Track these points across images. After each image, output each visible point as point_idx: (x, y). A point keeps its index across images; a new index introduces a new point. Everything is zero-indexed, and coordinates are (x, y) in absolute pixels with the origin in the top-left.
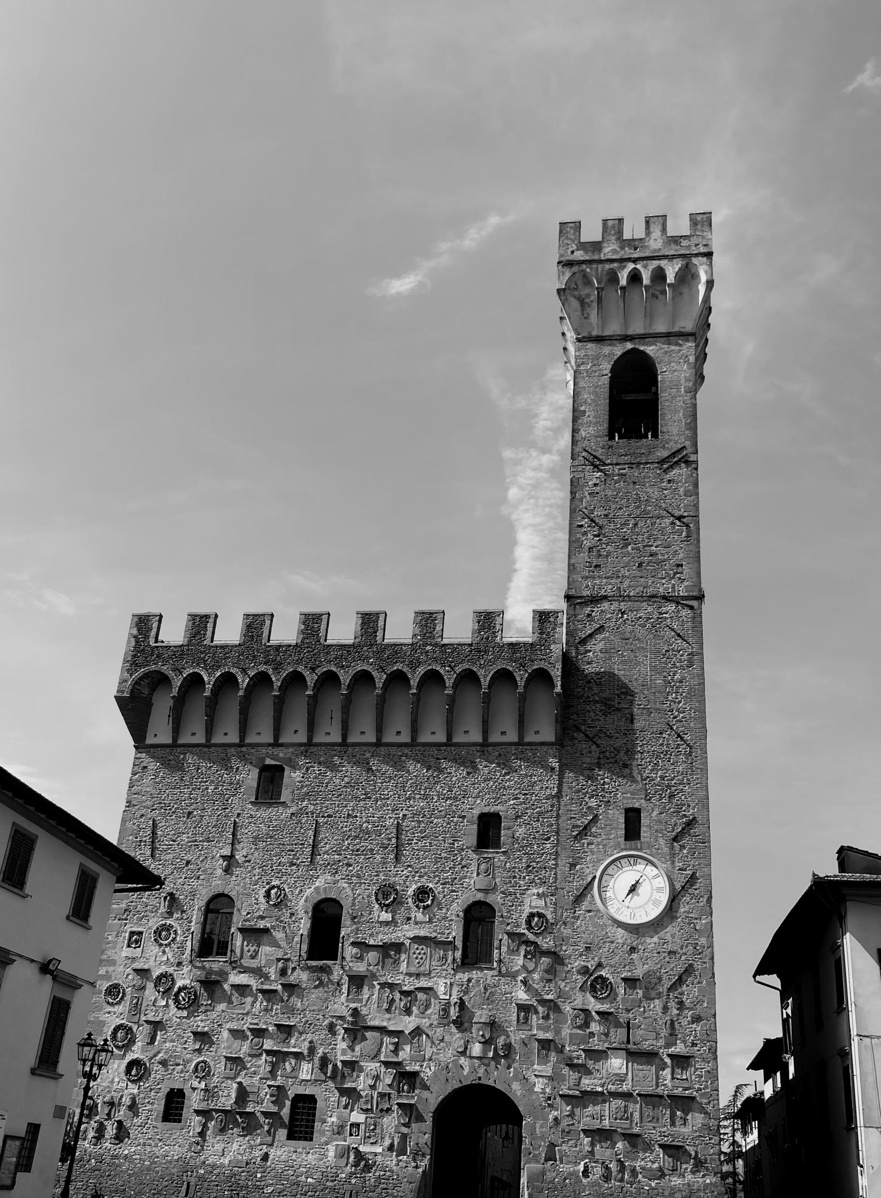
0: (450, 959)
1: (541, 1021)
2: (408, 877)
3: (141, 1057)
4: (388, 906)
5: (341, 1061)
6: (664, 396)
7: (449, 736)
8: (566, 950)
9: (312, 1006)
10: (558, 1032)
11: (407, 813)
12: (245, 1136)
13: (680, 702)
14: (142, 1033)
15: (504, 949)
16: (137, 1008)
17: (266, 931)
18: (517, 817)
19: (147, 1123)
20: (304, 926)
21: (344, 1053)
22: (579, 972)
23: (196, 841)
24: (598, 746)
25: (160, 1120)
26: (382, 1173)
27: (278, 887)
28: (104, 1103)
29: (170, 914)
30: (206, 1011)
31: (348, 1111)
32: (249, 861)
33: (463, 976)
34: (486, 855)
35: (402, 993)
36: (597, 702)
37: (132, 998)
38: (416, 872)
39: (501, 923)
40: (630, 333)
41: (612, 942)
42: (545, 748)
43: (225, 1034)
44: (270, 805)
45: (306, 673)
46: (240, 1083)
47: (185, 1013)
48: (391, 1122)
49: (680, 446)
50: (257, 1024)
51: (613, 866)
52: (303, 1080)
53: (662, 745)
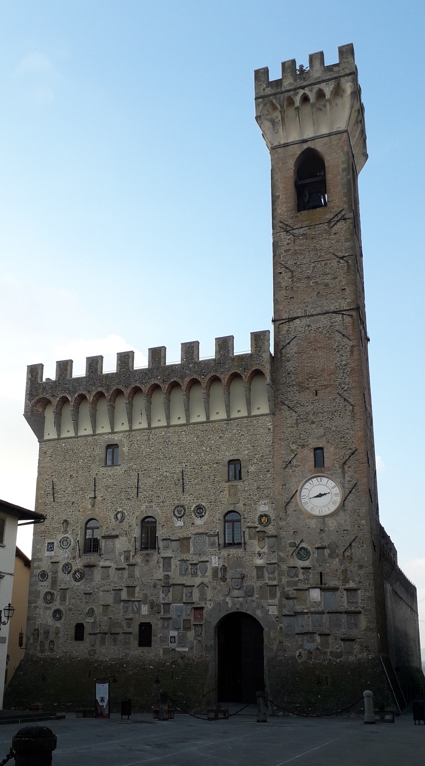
5: (162, 604)
6: (329, 176)
7: (208, 417)
13: (345, 378)
20: (137, 532)
21: (164, 599)
24: (296, 412)
27: (121, 512)
29: (66, 531)
32: (104, 499)
33: (225, 552)
35: (191, 564)
36: (294, 385)
37: (52, 578)
39: (245, 522)
40: (305, 137)
42: (264, 418)
45: (123, 390)
49: (340, 209)
51: (308, 483)
53: (335, 406)
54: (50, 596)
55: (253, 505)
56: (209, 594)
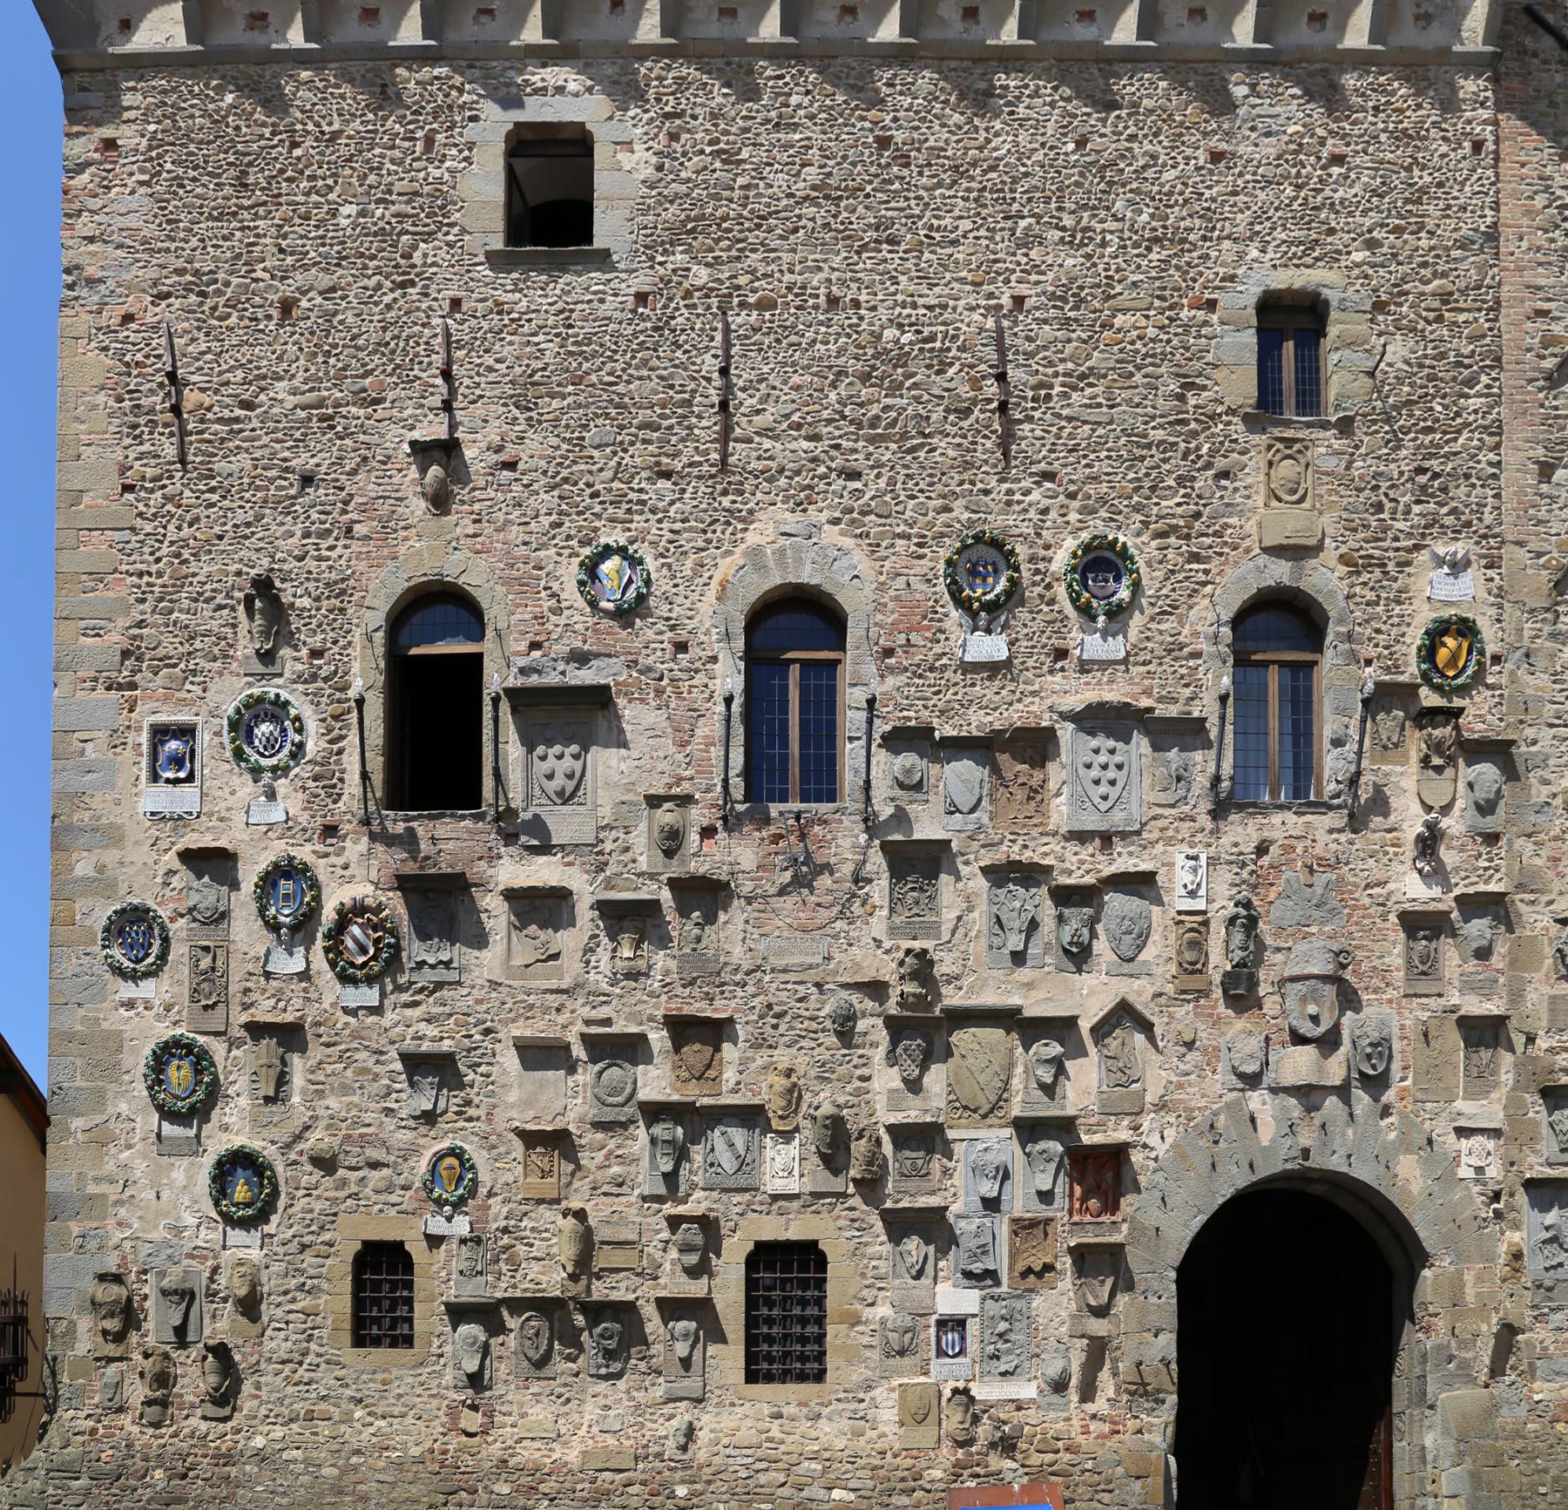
0: (1201, 781)
1: (1472, 965)
2: (1045, 511)
3: (257, 1145)
4: (993, 607)
5: (890, 1129)
9: (781, 953)
10: (1516, 996)
11: (1023, 290)
12: (619, 1376)
14: (239, 1069)
16: (209, 987)
17: (599, 698)
18: (1380, 307)
19: (305, 1354)
23: (320, 404)
25: (347, 1337)
26: (1049, 1457)
27: (622, 551)
28: (165, 1293)
30: (439, 986)
31: (926, 1281)
32: (511, 465)
33: (1242, 832)
34: (1289, 434)
38: (1072, 496)
43: (510, 1060)
44: (558, 266)
46: (580, 1215)
47: (370, 996)
48: (1057, 1304)
50: (607, 1022)
52: (776, 1198)
54: (186, 1063)
55: (1391, 567)
56: (1156, 1075)
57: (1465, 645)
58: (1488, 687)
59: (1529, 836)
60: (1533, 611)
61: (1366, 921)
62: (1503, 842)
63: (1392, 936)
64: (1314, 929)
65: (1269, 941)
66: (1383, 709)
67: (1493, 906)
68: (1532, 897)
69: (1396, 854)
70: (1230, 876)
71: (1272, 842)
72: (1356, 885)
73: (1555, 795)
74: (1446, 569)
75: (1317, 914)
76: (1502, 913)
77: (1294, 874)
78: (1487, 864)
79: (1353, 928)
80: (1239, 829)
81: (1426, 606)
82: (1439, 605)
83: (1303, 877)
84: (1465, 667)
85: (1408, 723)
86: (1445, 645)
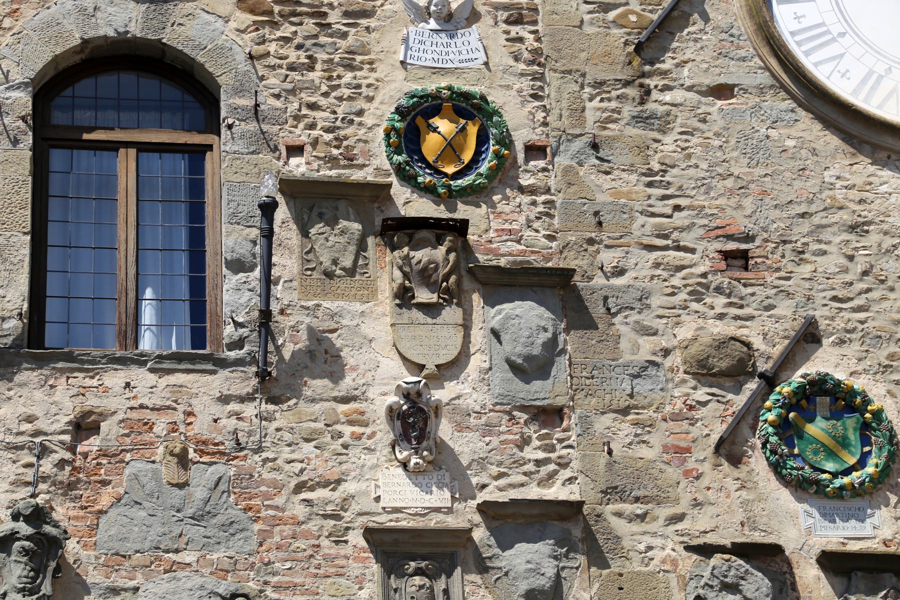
8: (621, 269)
15: (286, 264)
22: (703, 371)
41: (857, 228)
55: (334, 17)
57: (473, 130)
58: (522, 190)
59: (625, 412)
60: (599, 84)
61: (301, 544)
62: (572, 420)
63: (355, 569)
64: (188, 557)
65: (93, 577)
66: (321, 217)
67: (562, 523)
68: (639, 508)
69: (359, 437)
70: (11, 471)
71: (103, 416)
72: (278, 487)
73: (666, 352)
74: (433, 24)
75: (194, 532)
76: (577, 532)
77: (151, 468)
78: (541, 455)
79: (272, 556)
80: (39, 395)
81: (400, 74)
82: (422, 73)
83: (169, 471)
84: (476, 160)
85: (371, 241)
86: (435, 130)
